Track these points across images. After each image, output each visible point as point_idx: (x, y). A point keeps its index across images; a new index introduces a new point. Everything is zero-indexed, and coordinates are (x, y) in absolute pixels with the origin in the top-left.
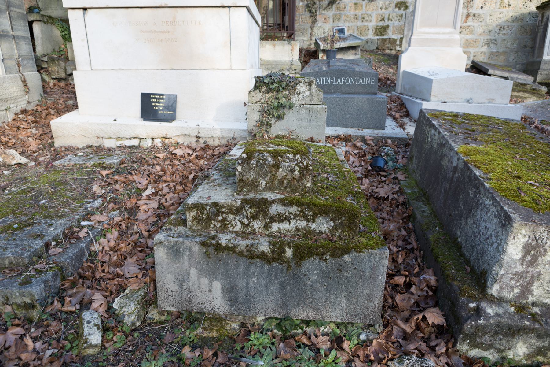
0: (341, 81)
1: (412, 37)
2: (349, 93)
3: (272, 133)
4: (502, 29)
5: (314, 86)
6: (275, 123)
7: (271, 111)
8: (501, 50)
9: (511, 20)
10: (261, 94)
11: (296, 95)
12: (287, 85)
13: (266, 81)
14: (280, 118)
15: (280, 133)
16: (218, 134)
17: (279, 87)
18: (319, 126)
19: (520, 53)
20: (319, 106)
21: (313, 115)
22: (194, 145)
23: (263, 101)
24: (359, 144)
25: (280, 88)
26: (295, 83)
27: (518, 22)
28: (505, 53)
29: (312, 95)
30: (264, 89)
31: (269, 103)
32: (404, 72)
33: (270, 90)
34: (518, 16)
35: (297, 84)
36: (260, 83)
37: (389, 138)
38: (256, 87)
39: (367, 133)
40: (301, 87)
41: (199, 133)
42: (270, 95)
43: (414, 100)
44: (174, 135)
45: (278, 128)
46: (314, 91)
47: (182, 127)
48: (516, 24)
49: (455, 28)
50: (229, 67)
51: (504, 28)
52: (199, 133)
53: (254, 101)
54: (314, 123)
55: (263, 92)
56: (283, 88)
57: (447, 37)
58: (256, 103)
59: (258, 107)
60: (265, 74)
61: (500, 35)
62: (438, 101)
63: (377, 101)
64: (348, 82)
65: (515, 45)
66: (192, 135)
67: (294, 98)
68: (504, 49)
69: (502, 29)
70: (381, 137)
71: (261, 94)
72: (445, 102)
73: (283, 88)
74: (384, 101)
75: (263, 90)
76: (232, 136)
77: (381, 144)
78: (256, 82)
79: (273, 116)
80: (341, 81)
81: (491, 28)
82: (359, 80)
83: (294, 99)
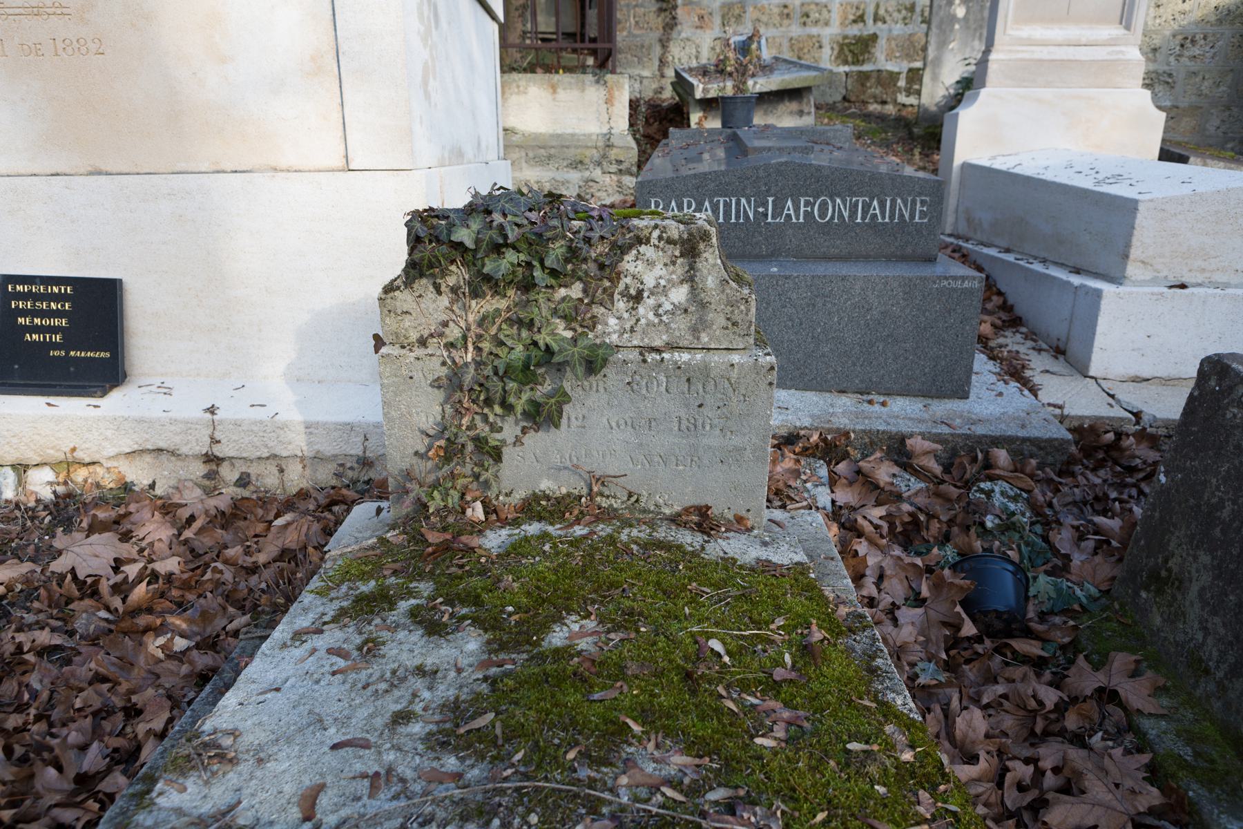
0: (797, 209)
1: (993, 57)
2: (827, 258)
3: (506, 486)
4: (1188, 44)
5: (711, 259)
6: (518, 441)
7: (496, 386)
8: (1184, 103)
9: (1213, 19)
10: (444, 301)
11: (621, 305)
12: (573, 254)
13: (464, 235)
14: (542, 416)
15: (545, 485)
16: (298, 443)
17: (529, 265)
18: (740, 450)
19: (1235, 110)
20: (736, 358)
21: (709, 401)
22: (192, 498)
23: (454, 333)
24: (884, 473)
25: (538, 273)
26: (614, 245)
27: (1232, 23)
28: (1194, 109)
29: (703, 305)
30: (457, 275)
31: (486, 346)
32: (966, 167)
33: (483, 284)
34: (1233, 8)
35: (624, 250)
36: (433, 243)
37: (997, 441)
38: (415, 269)
39: (903, 413)
40: (648, 268)
41: (215, 441)
42: (491, 303)
43: (1037, 267)
44: (112, 451)
45: (533, 464)
46: (711, 282)
47: (140, 421)
48: (1227, 30)
49: (1128, 28)
50: (340, 163)
51: (1193, 42)
52: (215, 441)
53: (414, 336)
54: (712, 439)
55: (454, 290)
56: (554, 273)
57: (1100, 53)
58: (423, 342)
59: (433, 364)
60: (458, 200)
61: (1183, 60)
62: (1154, 281)
63: (941, 291)
64: (823, 214)
65: (1222, 88)
66: (184, 450)
67: (612, 321)
68: (1194, 98)
69: (1188, 44)
70: (968, 437)
71: (444, 301)
72: (1183, 286)
73: (554, 273)
74: (970, 291)
75: (451, 281)
76: (357, 451)
77: (971, 470)
78: (415, 241)
79: (508, 408)
80: (797, 209)
81: (1157, 42)
82: (867, 207)
83: (611, 325)
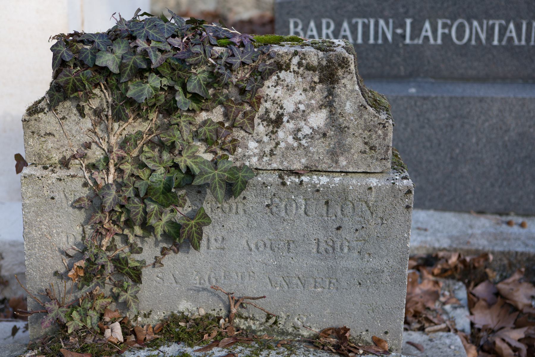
2: (464, 79)
5: (349, 85)
6: (157, 263)
7: (136, 207)
10: (87, 123)
11: (261, 129)
12: (214, 79)
13: (108, 60)
14: (181, 238)
15: (184, 306)
17: (171, 89)
18: (378, 272)
20: (373, 181)
21: (348, 223)
23: (96, 154)
25: (180, 98)
26: (255, 71)
29: (342, 130)
30: (101, 98)
31: (127, 167)
33: (126, 107)
35: (264, 75)
36: (77, 66)
38: (62, 91)
40: (287, 93)
42: (134, 126)
46: (349, 107)
53: (56, 157)
54: (351, 262)
55: (97, 113)
56: (195, 97)
58: (65, 163)
64: (460, 36)
67: (252, 145)
71: (87, 123)
73: (195, 97)
75: (95, 103)
78: (60, 65)
79: (149, 229)
82: (503, 30)
83: (252, 148)
